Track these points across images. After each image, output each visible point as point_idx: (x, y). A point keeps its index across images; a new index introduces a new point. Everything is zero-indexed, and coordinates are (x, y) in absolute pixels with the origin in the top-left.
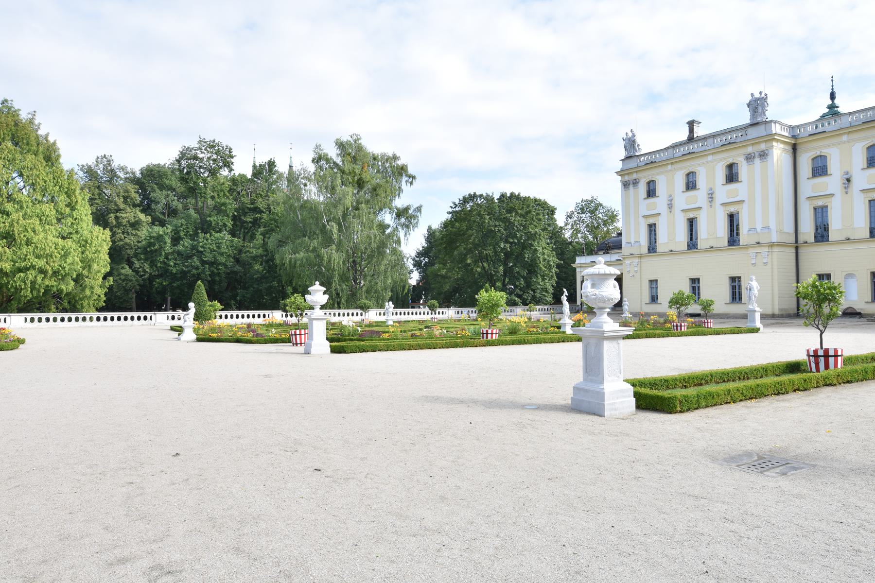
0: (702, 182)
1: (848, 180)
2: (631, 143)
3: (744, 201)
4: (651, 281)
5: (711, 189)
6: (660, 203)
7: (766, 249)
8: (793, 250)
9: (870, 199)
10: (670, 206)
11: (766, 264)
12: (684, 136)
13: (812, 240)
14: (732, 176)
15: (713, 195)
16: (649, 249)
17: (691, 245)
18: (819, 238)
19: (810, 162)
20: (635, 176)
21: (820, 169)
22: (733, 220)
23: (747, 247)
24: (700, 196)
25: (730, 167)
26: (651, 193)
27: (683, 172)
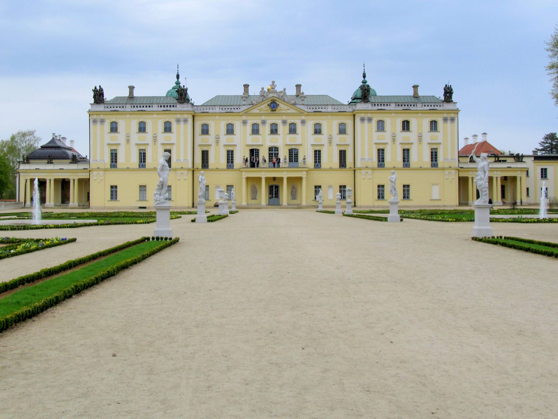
0: (149, 128)
2: (99, 96)
4: (112, 187)
5: (155, 134)
6: (120, 137)
7: (186, 172)
8: (191, 172)
10: (128, 140)
11: (185, 179)
12: (126, 94)
13: (200, 167)
14: (168, 128)
16: (111, 166)
17: (141, 166)
19: (201, 126)
20: (102, 117)
21: (205, 131)
23: (175, 170)
24: (147, 137)
25: (166, 123)
26: (114, 129)
27: (137, 120)
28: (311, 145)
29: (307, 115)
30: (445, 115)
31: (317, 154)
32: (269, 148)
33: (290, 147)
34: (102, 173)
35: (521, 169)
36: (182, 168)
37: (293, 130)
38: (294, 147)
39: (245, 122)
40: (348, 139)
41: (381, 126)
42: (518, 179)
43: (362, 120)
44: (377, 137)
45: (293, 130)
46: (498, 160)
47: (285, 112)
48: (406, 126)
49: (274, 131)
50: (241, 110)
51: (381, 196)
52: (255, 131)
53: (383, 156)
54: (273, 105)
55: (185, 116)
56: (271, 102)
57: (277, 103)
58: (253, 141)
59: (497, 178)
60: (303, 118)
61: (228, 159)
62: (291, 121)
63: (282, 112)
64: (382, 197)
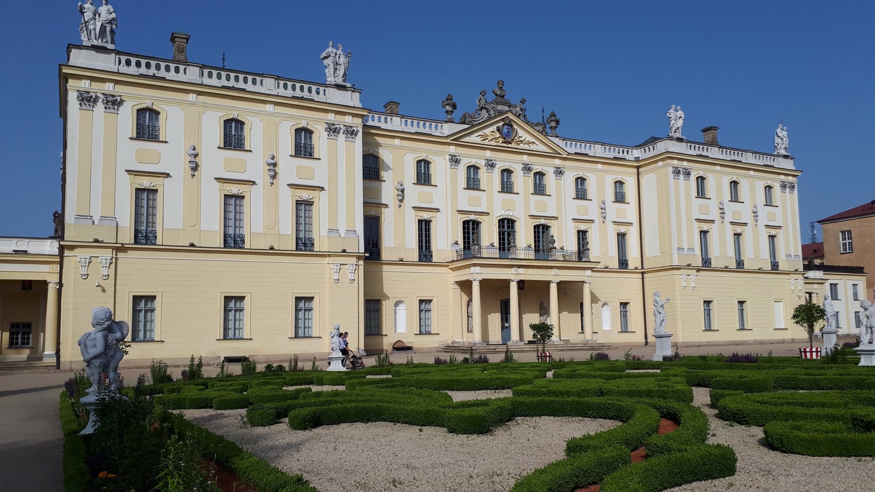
1: (403, 191)
3: (322, 189)
4: (137, 299)
9: (420, 218)
15: (276, 168)
28: (574, 219)
29: (565, 159)
32: (499, 221)
34: (108, 254)
38: (543, 221)
39: (455, 160)
40: (629, 211)
47: (527, 147)
54: (507, 134)
56: (502, 123)
57: (515, 126)
58: (468, 200)
60: (557, 162)
61: (420, 241)
62: (537, 167)
63: (521, 146)
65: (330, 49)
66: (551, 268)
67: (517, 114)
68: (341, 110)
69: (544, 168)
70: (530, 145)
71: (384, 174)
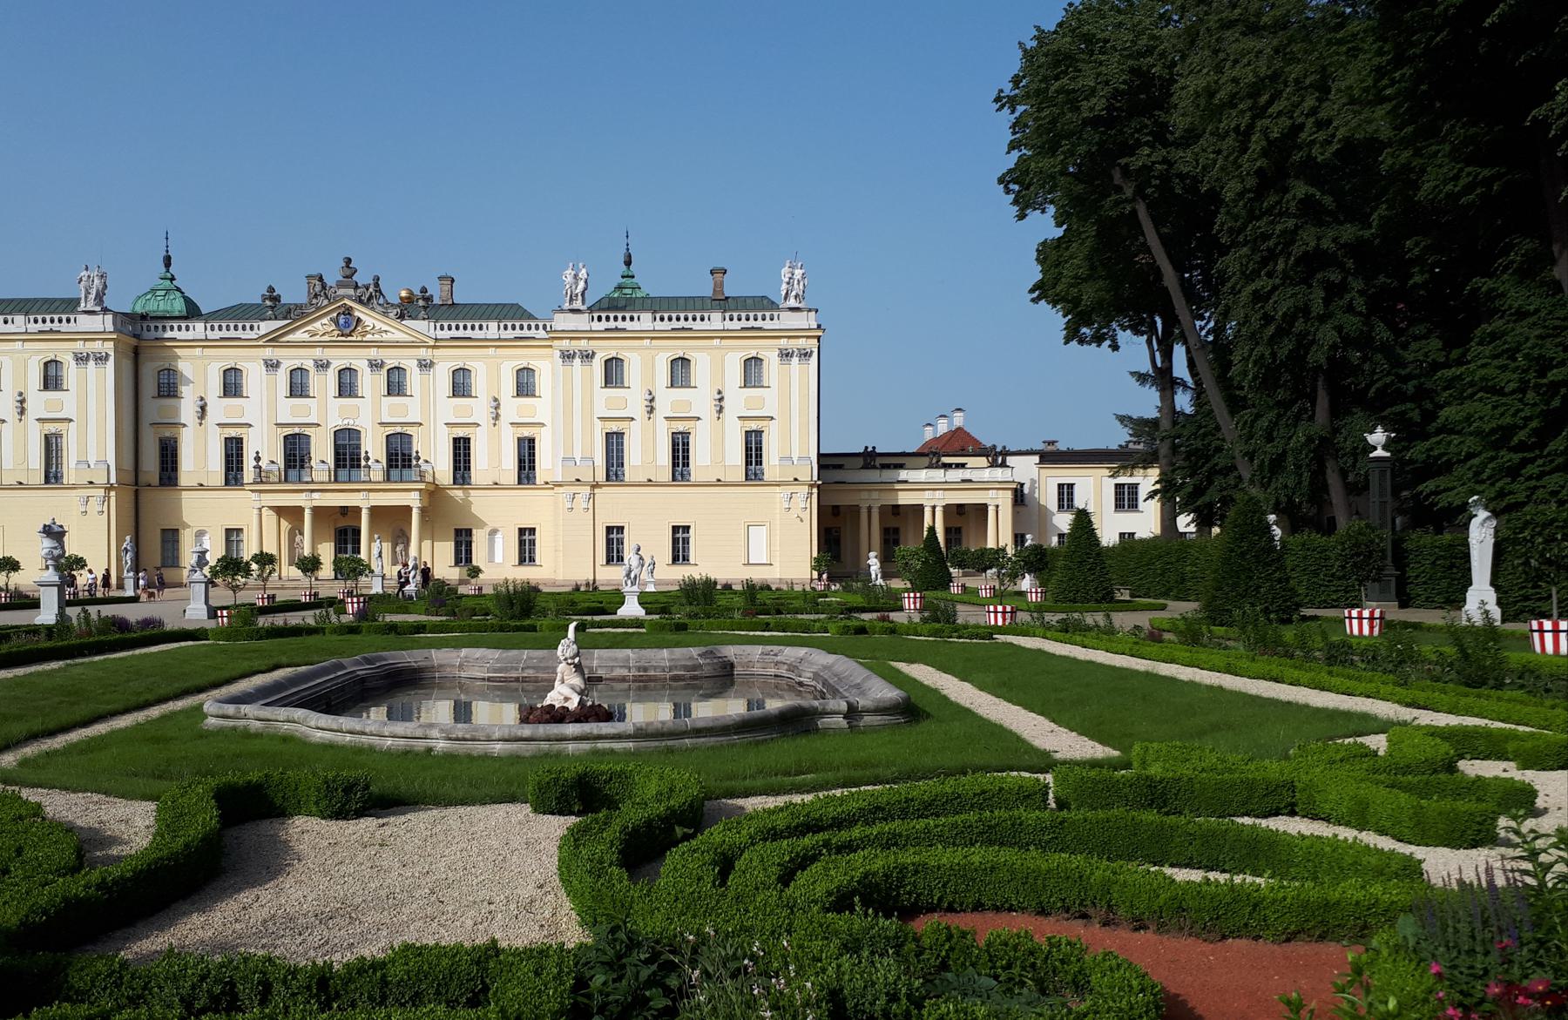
1: (203, 408)
3: (71, 420)
13: (155, 480)
18: (166, 481)
22: (52, 447)
23: (74, 487)
29: (434, 347)
30: (783, 342)
31: (461, 448)
33: (387, 429)
35: (1000, 486)
36: (91, 483)
37: (396, 385)
39: (272, 365)
41: (613, 373)
42: (991, 511)
43: (567, 356)
44: (605, 401)
45: (396, 385)
46: (938, 462)
47: (377, 337)
48: (680, 370)
49: (347, 385)
50: (262, 332)
51: (614, 554)
52: (298, 387)
53: (621, 451)
55: (97, 346)
57: (357, 314)
58: (292, 411)
59: (934, 508)
60: (422, 353)
63: (369, 337)
64: (618, 557)
65: (84, 273)
66: (358, 491)
67: (364, 298)
68: (88, 336)
69: (402, 362)
70: (384, 334)
71: (185, 390)
